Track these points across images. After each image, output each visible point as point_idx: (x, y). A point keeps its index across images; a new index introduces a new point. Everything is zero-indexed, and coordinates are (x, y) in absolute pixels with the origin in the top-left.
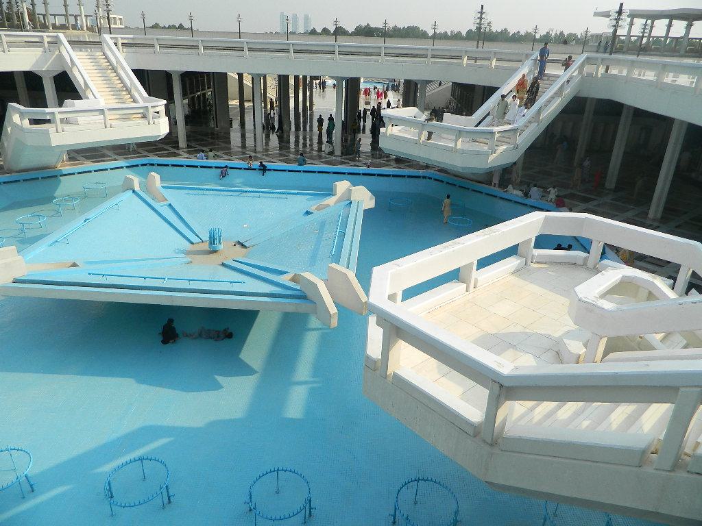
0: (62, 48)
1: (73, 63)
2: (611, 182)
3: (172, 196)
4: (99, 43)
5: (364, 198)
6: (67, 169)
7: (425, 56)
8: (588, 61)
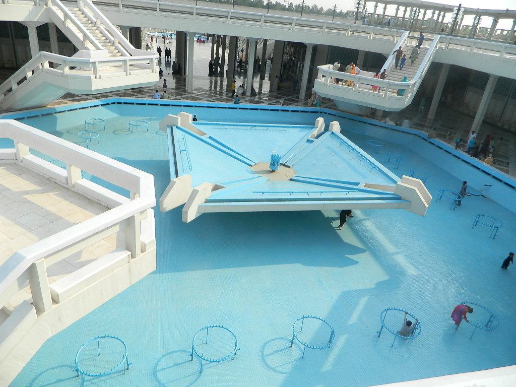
1: (66, 15)
3: (210, 131)
5: (336, 126)
6: (59, 108)
8: (440, 41)
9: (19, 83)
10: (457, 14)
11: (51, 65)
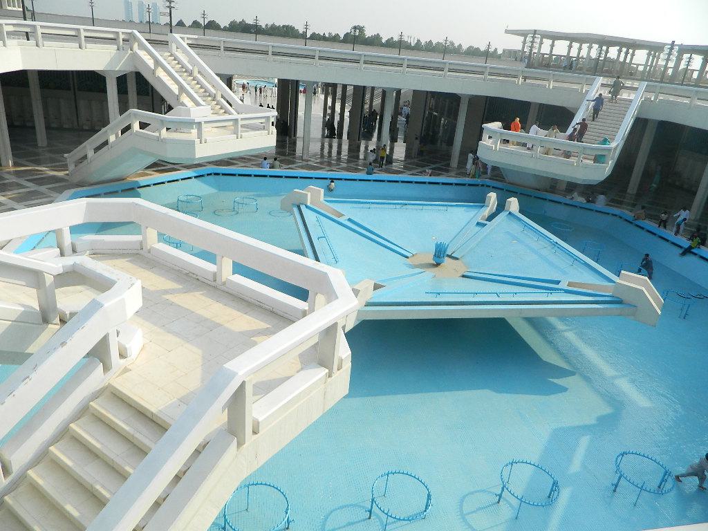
0: (136, 46)
1: (157, 63)
2: (633, 188)
3: (348, 211)
4: (165, 43)
5: (513, 204)
6: (143, 181)
7: (482, 73)
9: (97, 149)
10: (670, 54)
11: (143, 126)
